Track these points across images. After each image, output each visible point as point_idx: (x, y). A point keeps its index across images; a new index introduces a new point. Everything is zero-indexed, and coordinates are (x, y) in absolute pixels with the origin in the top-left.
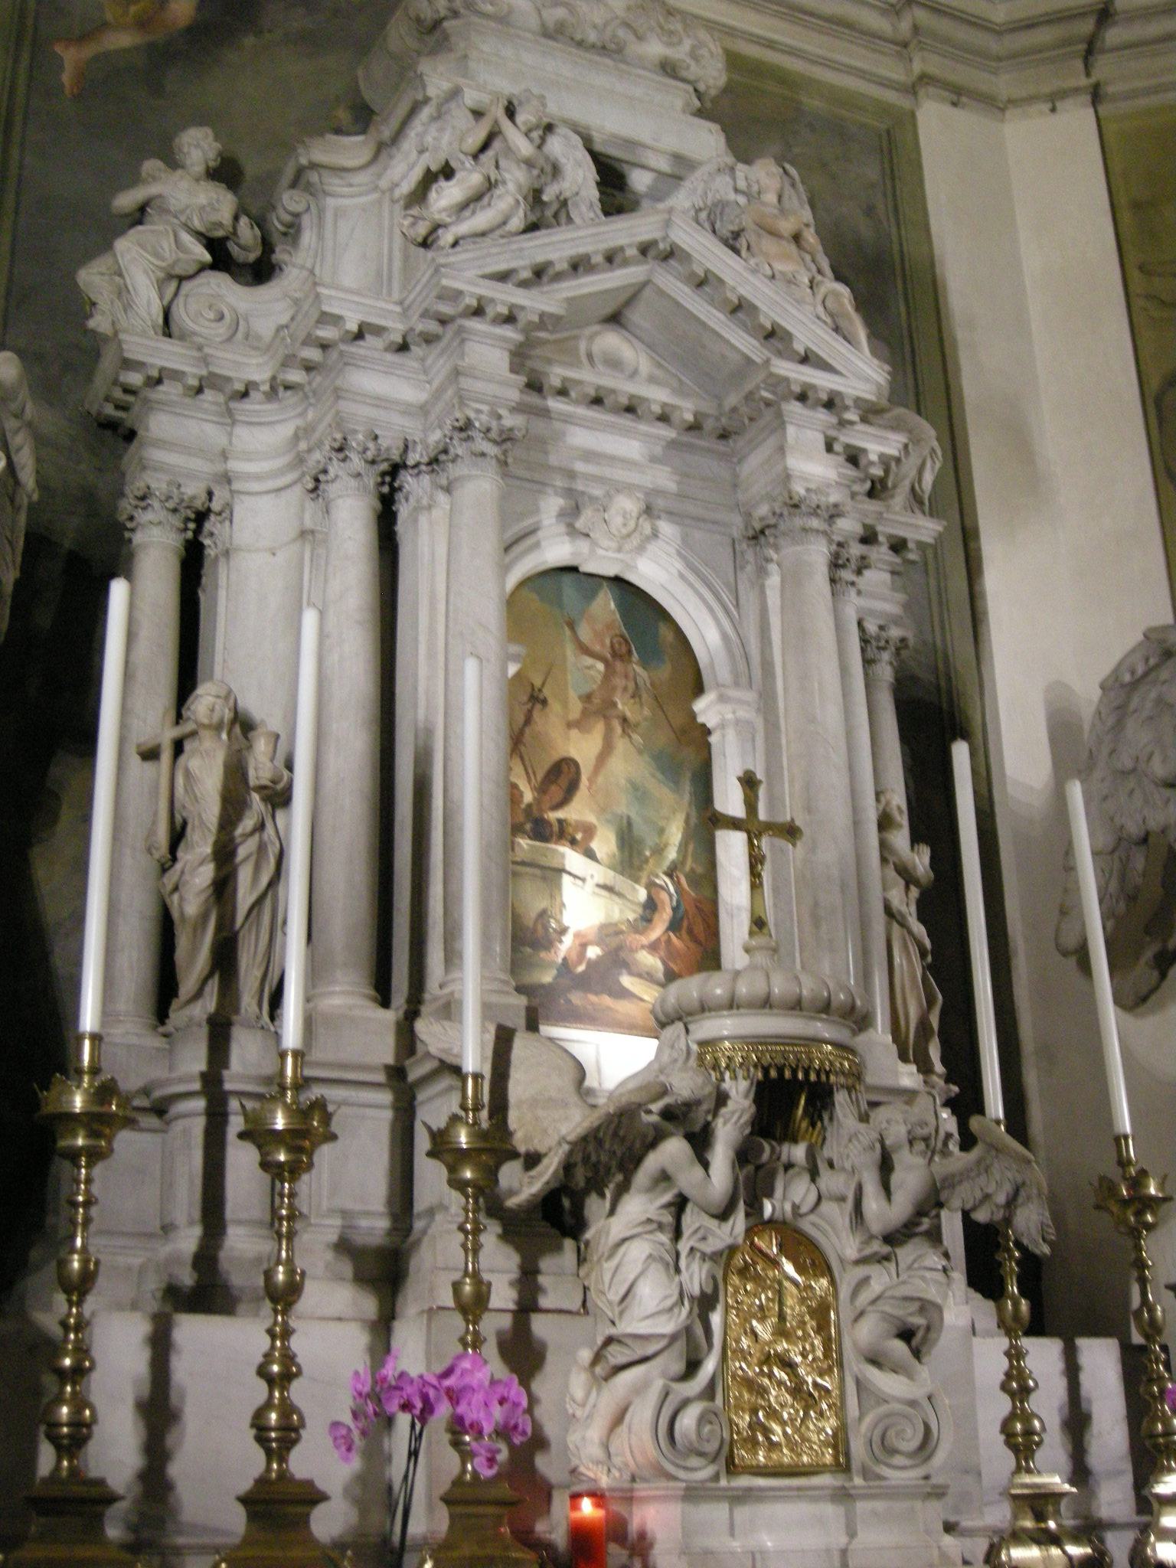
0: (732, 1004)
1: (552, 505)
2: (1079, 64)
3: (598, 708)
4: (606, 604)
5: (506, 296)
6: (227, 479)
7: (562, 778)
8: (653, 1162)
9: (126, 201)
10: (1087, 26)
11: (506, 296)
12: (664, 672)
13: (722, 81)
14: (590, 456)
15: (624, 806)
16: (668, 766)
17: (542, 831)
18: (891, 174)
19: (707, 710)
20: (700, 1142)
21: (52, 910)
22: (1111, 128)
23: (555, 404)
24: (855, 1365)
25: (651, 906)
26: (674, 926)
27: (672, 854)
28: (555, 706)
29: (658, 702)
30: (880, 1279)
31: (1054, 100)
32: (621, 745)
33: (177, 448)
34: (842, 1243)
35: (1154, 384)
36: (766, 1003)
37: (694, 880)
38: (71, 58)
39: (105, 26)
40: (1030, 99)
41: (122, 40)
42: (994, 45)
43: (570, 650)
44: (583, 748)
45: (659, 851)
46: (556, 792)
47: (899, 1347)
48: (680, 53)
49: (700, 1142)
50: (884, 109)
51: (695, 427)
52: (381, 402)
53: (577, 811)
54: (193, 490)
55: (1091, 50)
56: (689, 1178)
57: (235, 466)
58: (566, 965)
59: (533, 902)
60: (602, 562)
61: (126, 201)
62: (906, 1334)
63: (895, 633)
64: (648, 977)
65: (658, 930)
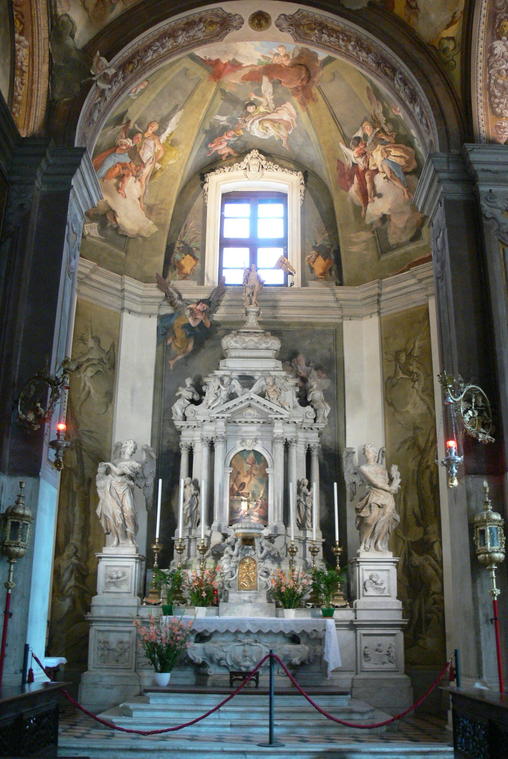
0: (242, 528)
1: (238, 442)
2: (376, 306)
3: (249, 473)
4: (252, 455)
5: (221, 415)
6: (193, 441)
7: (243, 485)
8: (226, 550)
9: (177, 394)
10: (376, 298)
11: (221, 415)
12: (262, 465)
13: (280, 346)
14: (245, 432)
15: (253, 489)
16: (261, 481)
17: (238, 495)
18: (335, 339)
19: (268, 471)
20: (233, 548)
21: (175, 510)
22: (383, 319)
23: (239, 424)
24: (259, 576)
25: (257, 505)
26: (261, 508)
27: (261, 496)
28: (242, 474)
29: (260, 470)
30: (262, 564)
31: (371, 315)
32: (253, 479)
33: (186, 438)
34: (257, 560)
35: (386, 379)
36: (246, 528)
37: (265, 500)
38: (172, 363)
39: (177, 355)
40: (367, 315)
41: (180, 357)
42: (360, 303)
43: (245, 464)
44: (246, 480)
45: (259, 495)
46: (241, 488)
47: (265, 574)
48: (269, 345)
49: (233, 548)
50: (335, 324)
51: (264, 423)
52: (209, 431)
53: (245, 491)
54: (189, 443)
55: (379, 302)
56: (231, 552)
57: (195, 439)
58: (241, 516)
59: (236, 506)
60: (248, 449)
61: (177, 394)
62: (266, 572)
63: (317, 445)
64: (256, 516)
65: (258, 508)
